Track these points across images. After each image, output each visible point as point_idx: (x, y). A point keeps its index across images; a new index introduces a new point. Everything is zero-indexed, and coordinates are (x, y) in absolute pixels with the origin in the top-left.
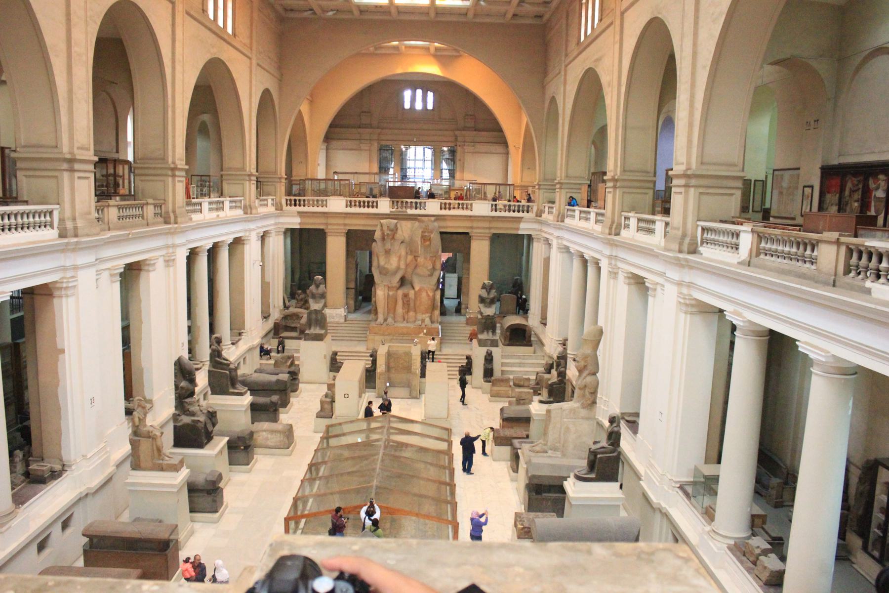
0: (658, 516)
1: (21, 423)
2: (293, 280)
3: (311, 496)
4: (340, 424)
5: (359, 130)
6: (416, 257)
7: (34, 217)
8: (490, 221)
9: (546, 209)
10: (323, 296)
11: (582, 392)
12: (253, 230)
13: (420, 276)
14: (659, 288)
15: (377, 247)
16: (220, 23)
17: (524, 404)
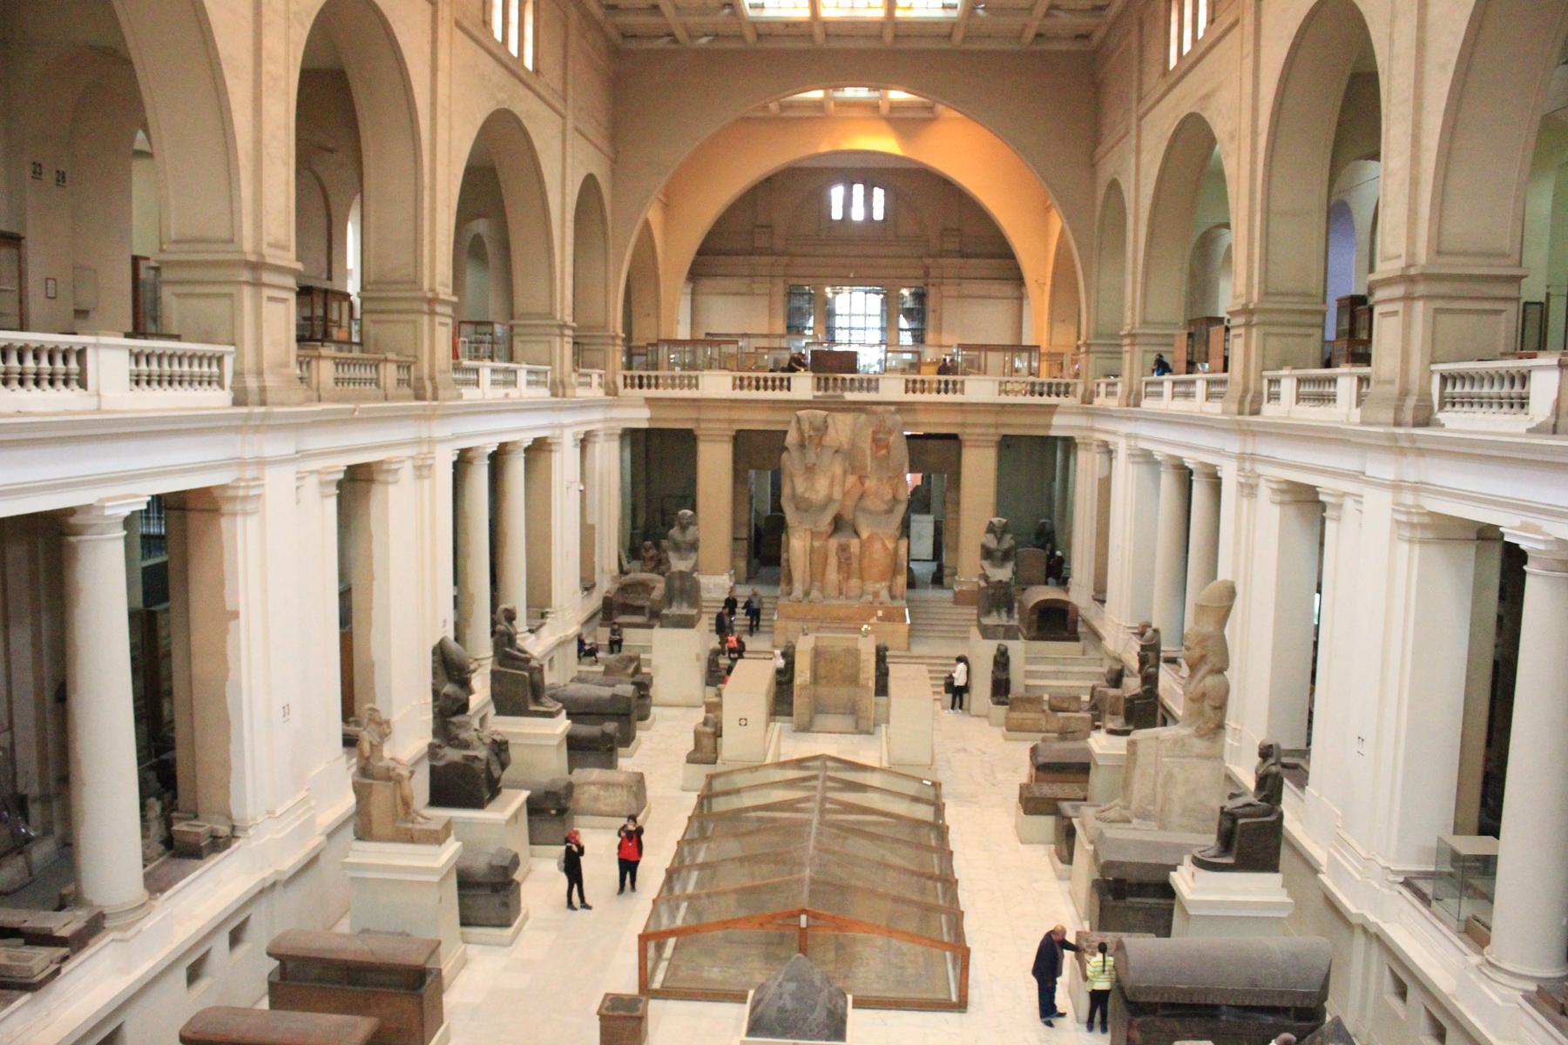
0: (1360, 940)
1: (157, 756)
2: (634, 527)
3: (690, 898)
4: (732, 772)
5: (755, 259)
6: (862, 479)
7: (190, 365)
8: (997, 413)
9: (1103, 388)
10: (693, 546)
11: (1197, 705)
12: (568, 427)
13: (871, 513)
14: (1349, 503)
15: (791, 461)
16: (513, 48)
17: (1075, 739)
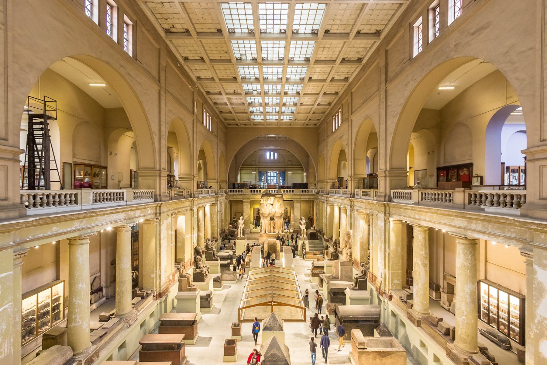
16: (208, 128)
